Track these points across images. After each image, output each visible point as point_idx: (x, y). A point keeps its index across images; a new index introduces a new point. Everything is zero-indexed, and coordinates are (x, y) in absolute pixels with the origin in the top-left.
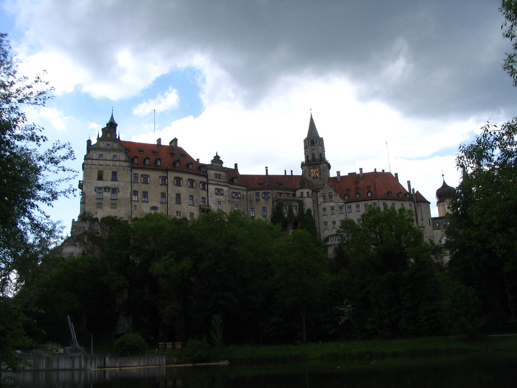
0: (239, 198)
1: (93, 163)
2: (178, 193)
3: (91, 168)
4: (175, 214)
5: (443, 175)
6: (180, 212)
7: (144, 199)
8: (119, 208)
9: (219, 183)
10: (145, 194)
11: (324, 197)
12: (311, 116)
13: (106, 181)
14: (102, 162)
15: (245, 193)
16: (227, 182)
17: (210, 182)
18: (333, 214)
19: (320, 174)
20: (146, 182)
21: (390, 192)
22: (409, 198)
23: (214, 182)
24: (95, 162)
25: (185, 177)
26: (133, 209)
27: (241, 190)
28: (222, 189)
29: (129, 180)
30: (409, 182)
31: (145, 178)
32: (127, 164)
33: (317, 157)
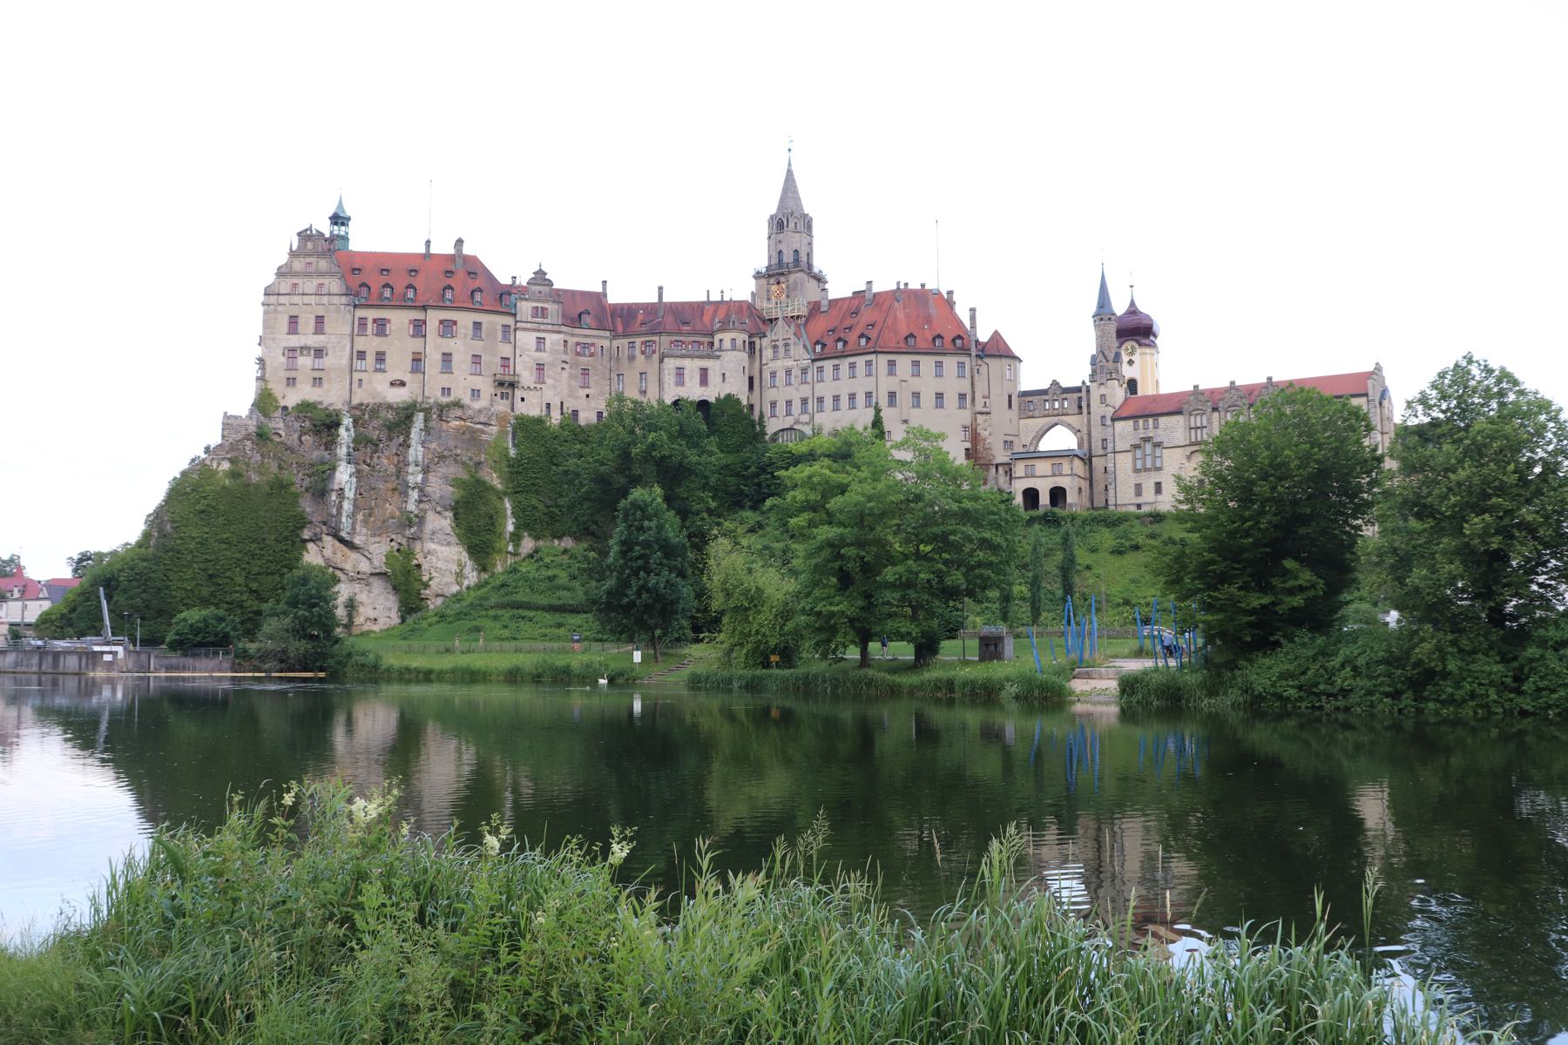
0: (592, 355)
2: (446, 351)
3: (276, 311)
4: (439, 394)
5: (1132, 286)
6: (449, 389)
7: (378, 366)
8: (326, 385)
9: (543, 327)
10: (380, 357)
11: (775, 347)
12: (790, 164)
14: (296, 299)
15: (606, 343)
17: (519, 325)
18: (789, 384)
19: (788, 296)
21: (911, 335)
22: (959, 349)
23: (529, 325)
24: (283, 299)
25: (465, 320)
26: (355, 385)
27: (598, 337)
29: (348, 330)
30: (973, 310)
31: (381, 325)
32: (344, 300)
33: (788, 258)
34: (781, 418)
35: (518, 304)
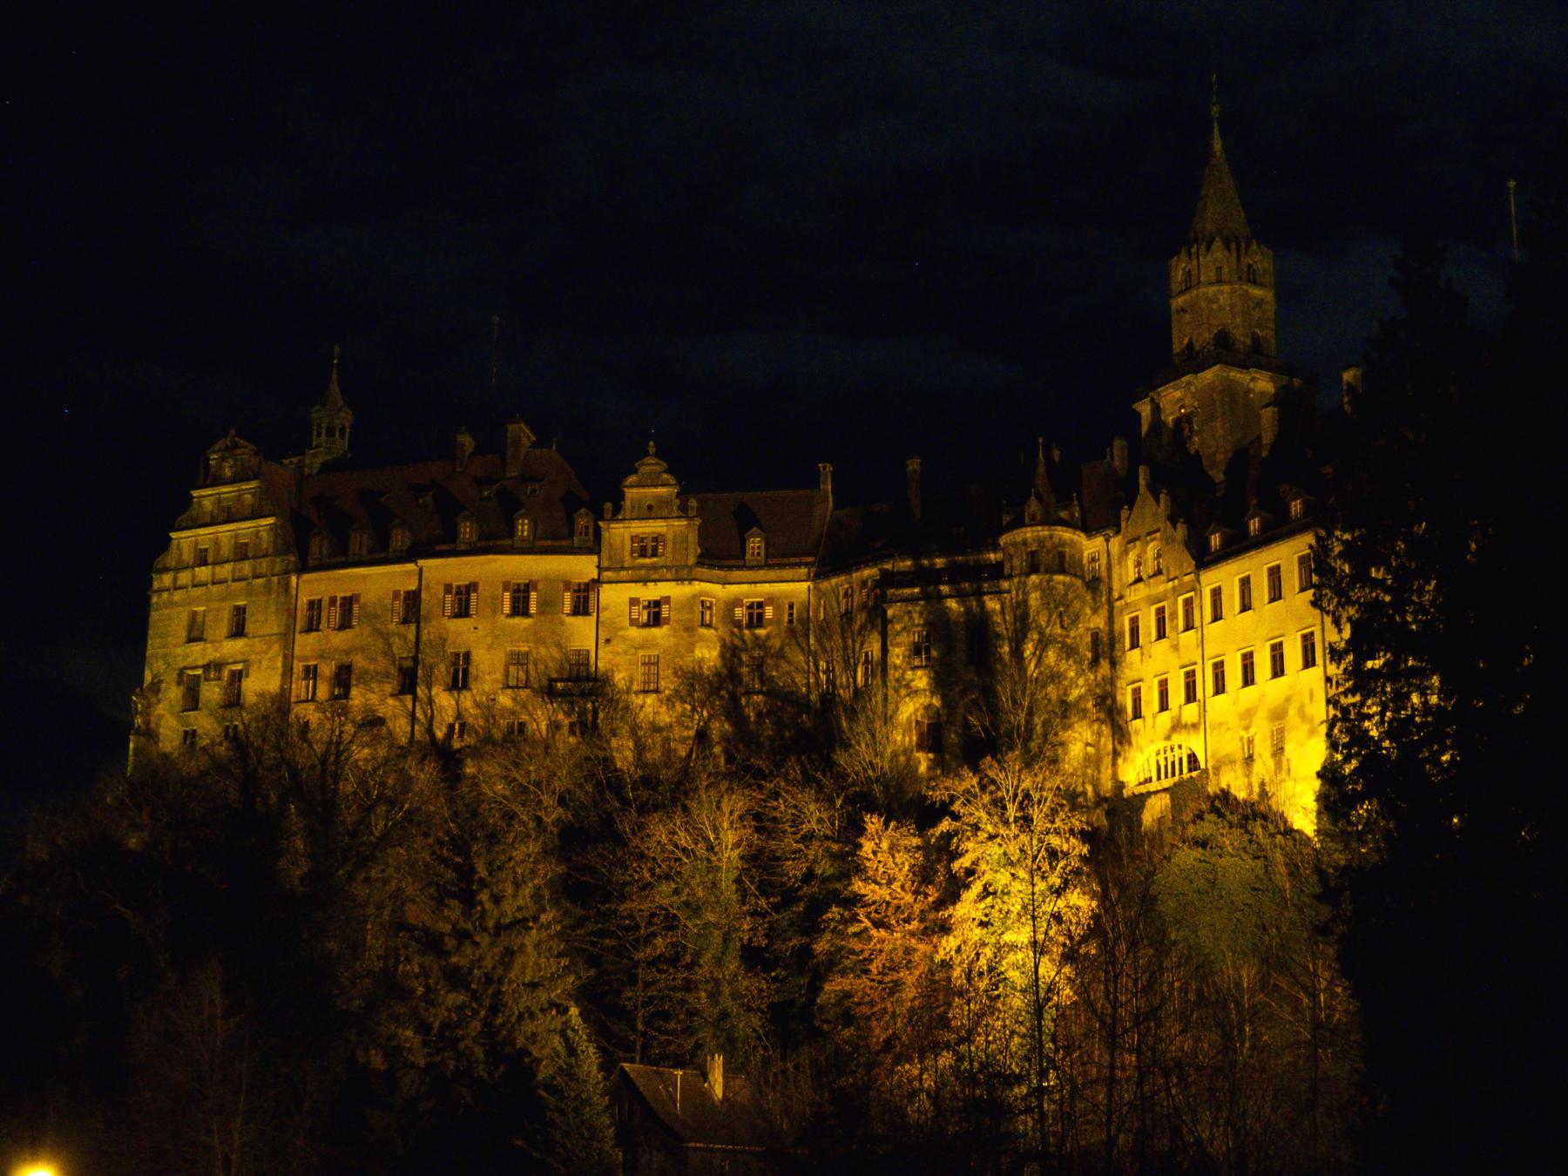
1: (179, 583)
13: (212, 642)
16: (691, 561)
24: (184, 577)
28: (667, 600)
34: (1149, 719)
35: (605, 535)
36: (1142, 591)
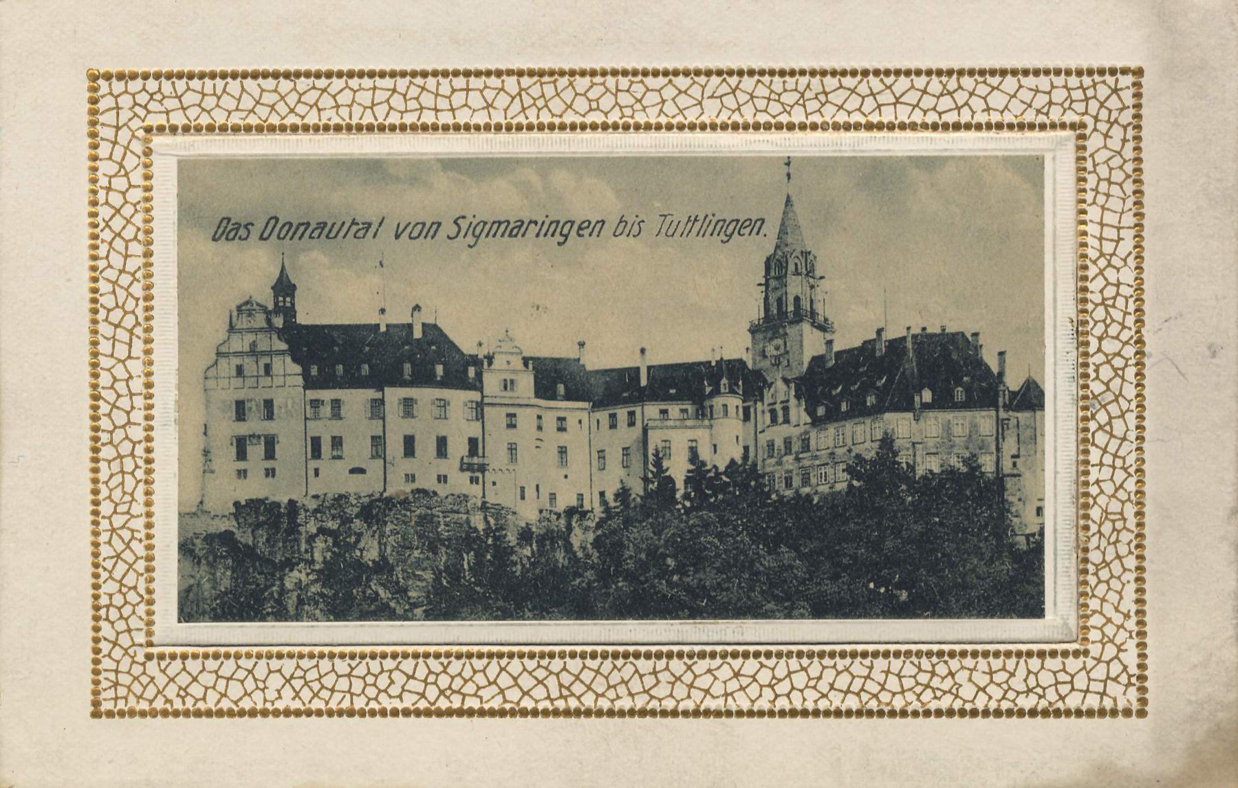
10: (337, 442)
11: (773, 413)
17: (486, 400)
20: (336, 414)
36: (776, 429)
